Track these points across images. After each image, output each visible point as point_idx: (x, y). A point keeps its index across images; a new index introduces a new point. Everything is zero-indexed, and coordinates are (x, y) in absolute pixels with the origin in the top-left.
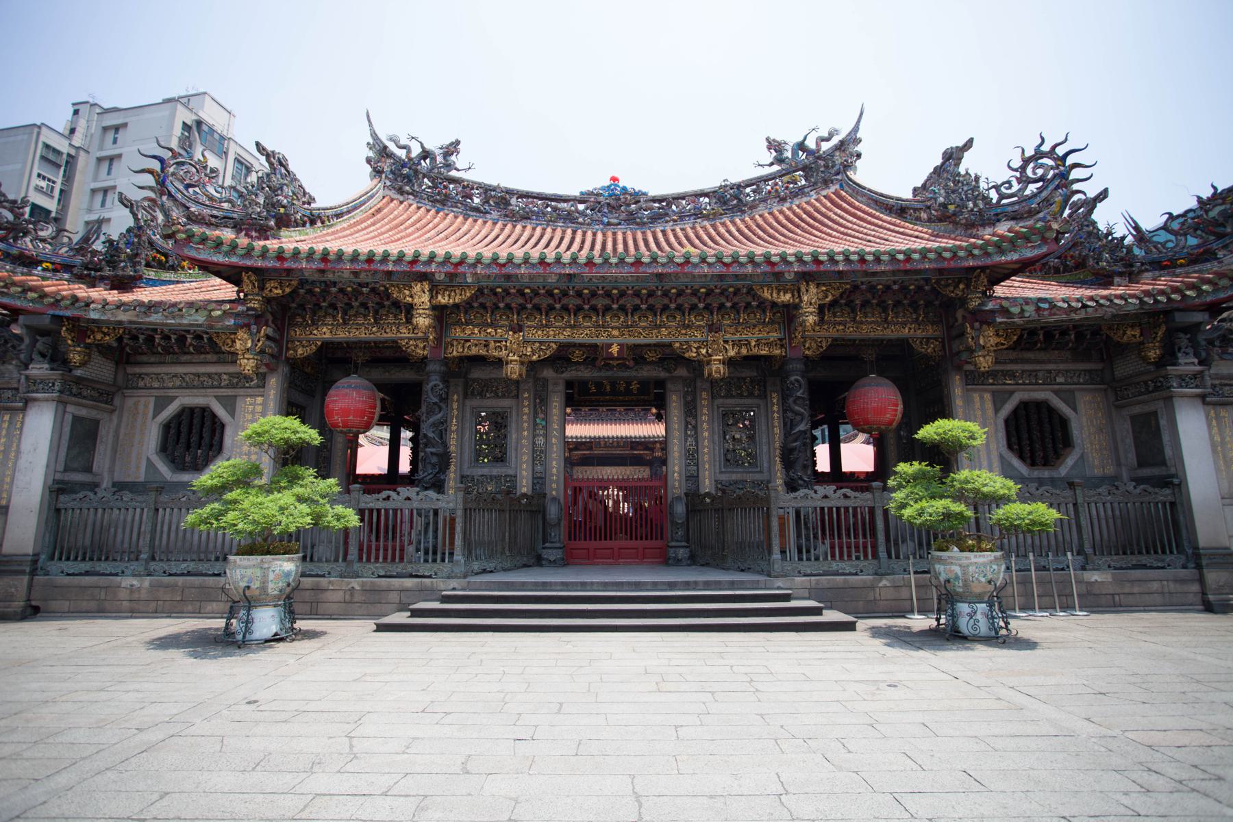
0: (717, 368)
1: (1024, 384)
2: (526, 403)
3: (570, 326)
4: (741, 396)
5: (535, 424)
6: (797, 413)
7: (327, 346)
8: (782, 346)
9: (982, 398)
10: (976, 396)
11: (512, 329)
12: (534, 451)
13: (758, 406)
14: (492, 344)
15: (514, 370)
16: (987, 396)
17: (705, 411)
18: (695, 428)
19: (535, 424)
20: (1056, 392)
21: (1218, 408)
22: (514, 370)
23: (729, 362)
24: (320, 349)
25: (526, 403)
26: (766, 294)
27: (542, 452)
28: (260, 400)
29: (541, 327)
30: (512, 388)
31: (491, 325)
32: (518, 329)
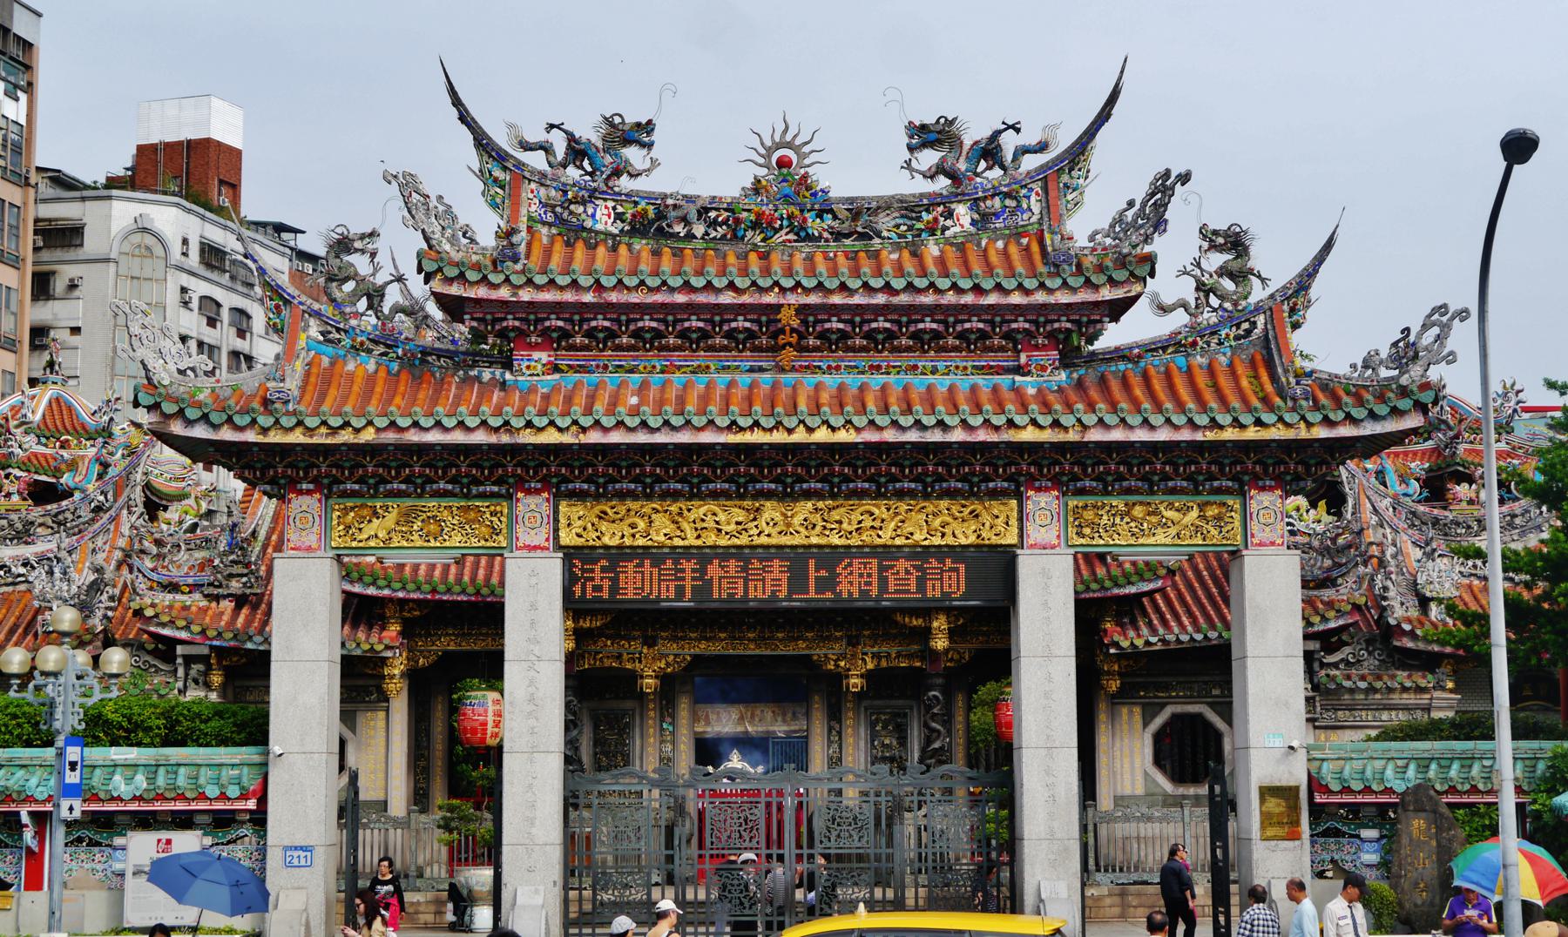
0: (855, 682)
1: (1177, 697)
2: (652, 706)
3: (707, 639)
4: (891, 697)
5: (662, 729)
6: (934, 730)
7: (446, 653)
8: (922, 659)
9: (1131, 713)
10: (1125, 710)
11: (645, 643)
12: (661, 760)
13: (911, 708)
14: (625, 656)
15: (649, 683)
16: (1137, 710)
17: (850, 714)
18: (840, 733)
19: (662, 729)
20: (1211, 705)
21: (1329, 732)
22: (649, 683)
23: (868, 676)
24: (440, 658)
25: (652, 706)
26: (899, 618)
27: (669, 760)
28: (382, 714)
29: (675, 639)
30: (642, 696)
31: (623, 638)
32: (650, 642)
